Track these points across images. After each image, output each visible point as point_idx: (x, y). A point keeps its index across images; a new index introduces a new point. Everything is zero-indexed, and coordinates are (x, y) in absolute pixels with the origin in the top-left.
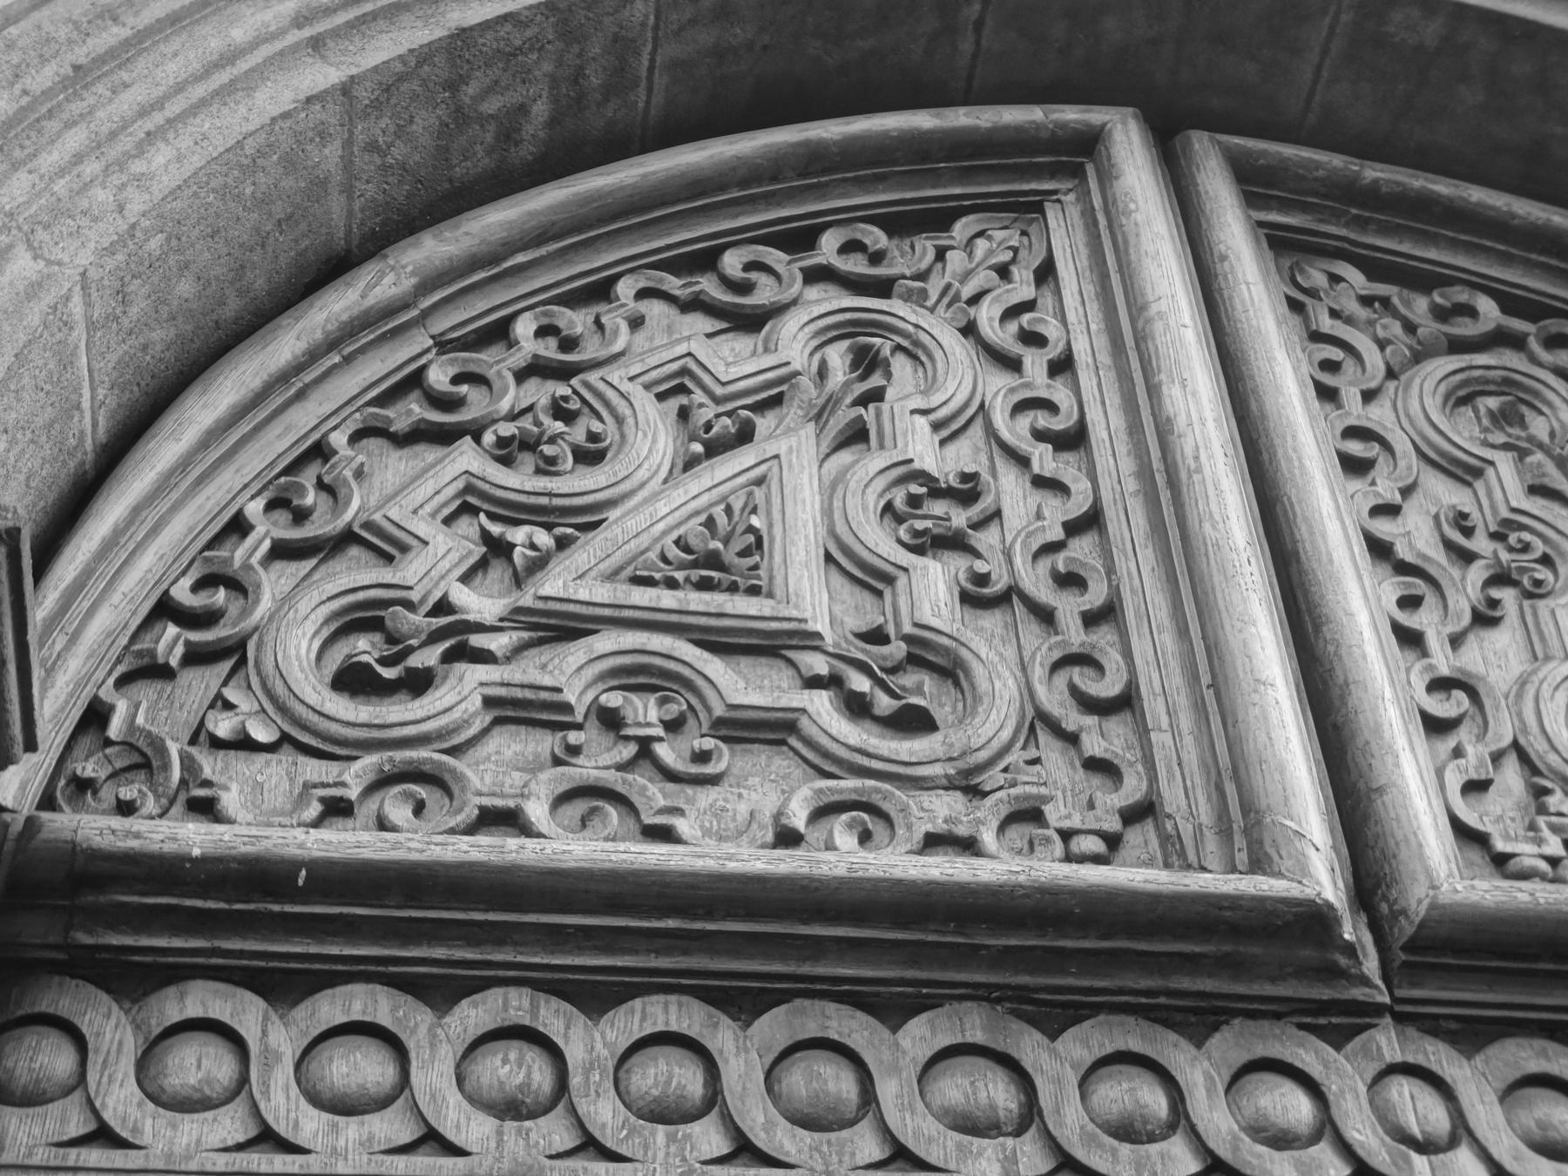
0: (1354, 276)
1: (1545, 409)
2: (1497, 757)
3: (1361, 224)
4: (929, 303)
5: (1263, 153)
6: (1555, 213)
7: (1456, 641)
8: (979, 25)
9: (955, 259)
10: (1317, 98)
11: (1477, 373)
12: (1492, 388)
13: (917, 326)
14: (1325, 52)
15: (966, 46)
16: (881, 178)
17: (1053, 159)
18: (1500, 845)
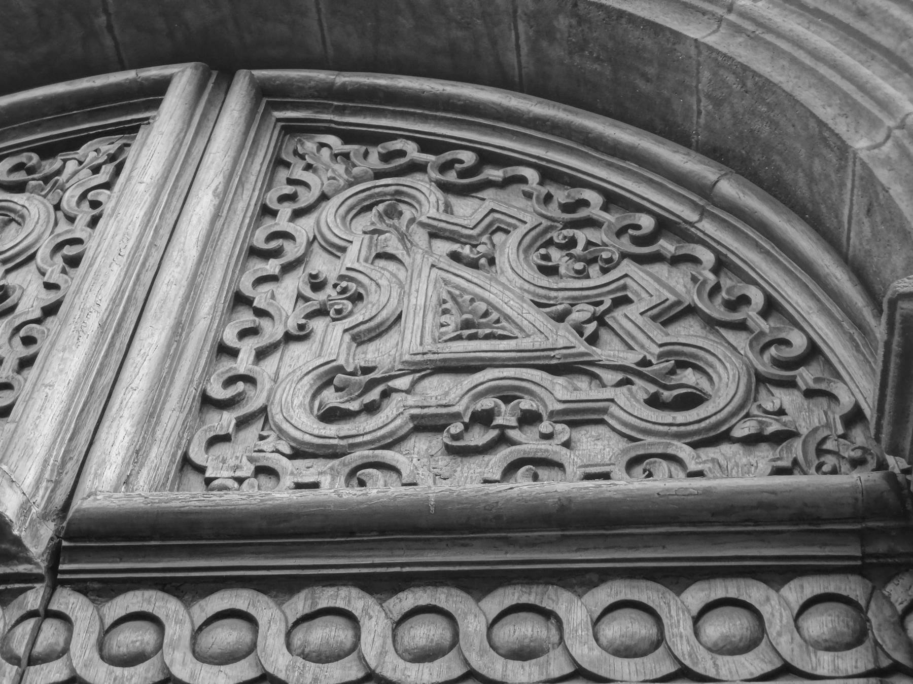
0: (332, 140)
1: (417, 206)
2: (243, 423)
3: (341, 111)
4: (43, 193)
5: (277, 78)
6: (448, 85)
7: (261, 354)
8: (110, 28)
9: (71, 166)
10: (328, 41)
11: (377, 190)
12: (389, 198)
13: (23, 206)
14: (319, 11)
15: (108, 42)
16: (38, 125)
17: (145, 99)
18: (208, 474)
